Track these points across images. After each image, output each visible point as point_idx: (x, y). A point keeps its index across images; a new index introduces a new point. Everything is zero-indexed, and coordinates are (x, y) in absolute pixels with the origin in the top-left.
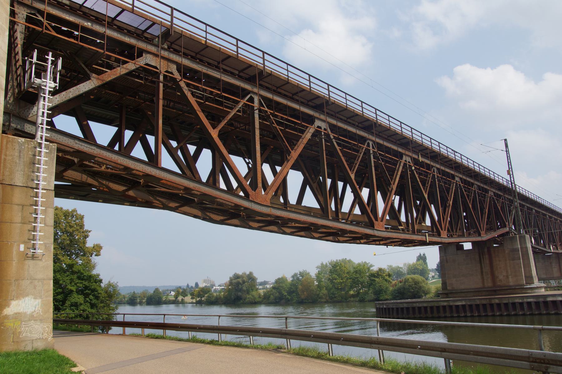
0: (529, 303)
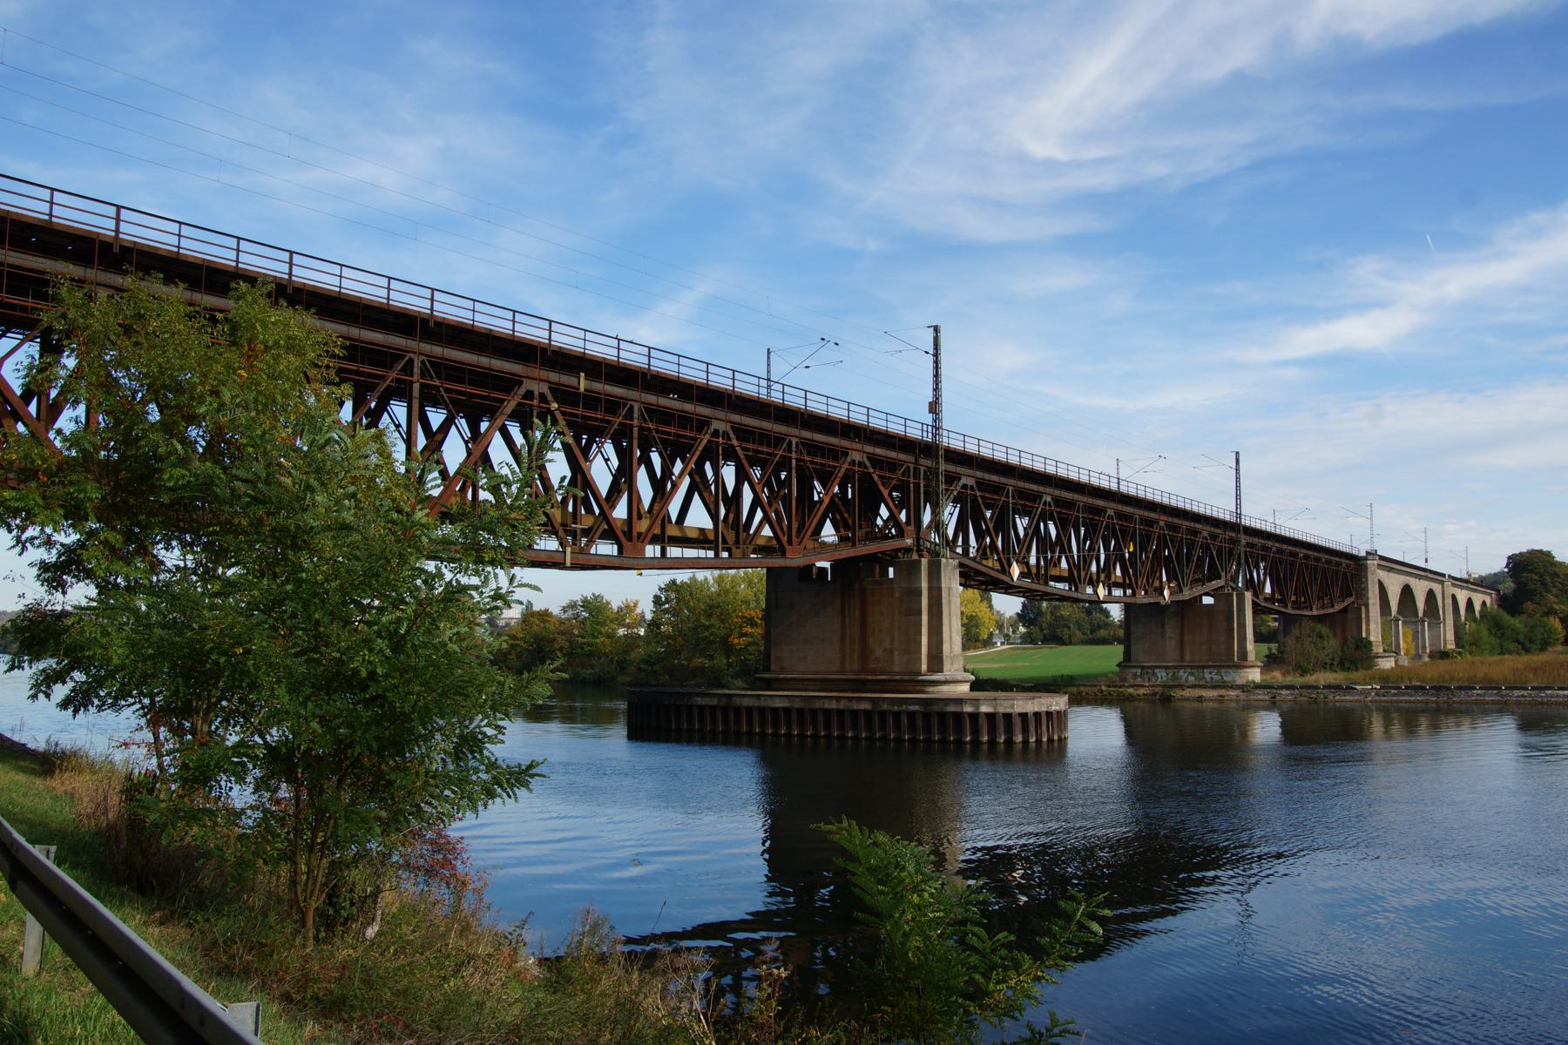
0: (912, 715)
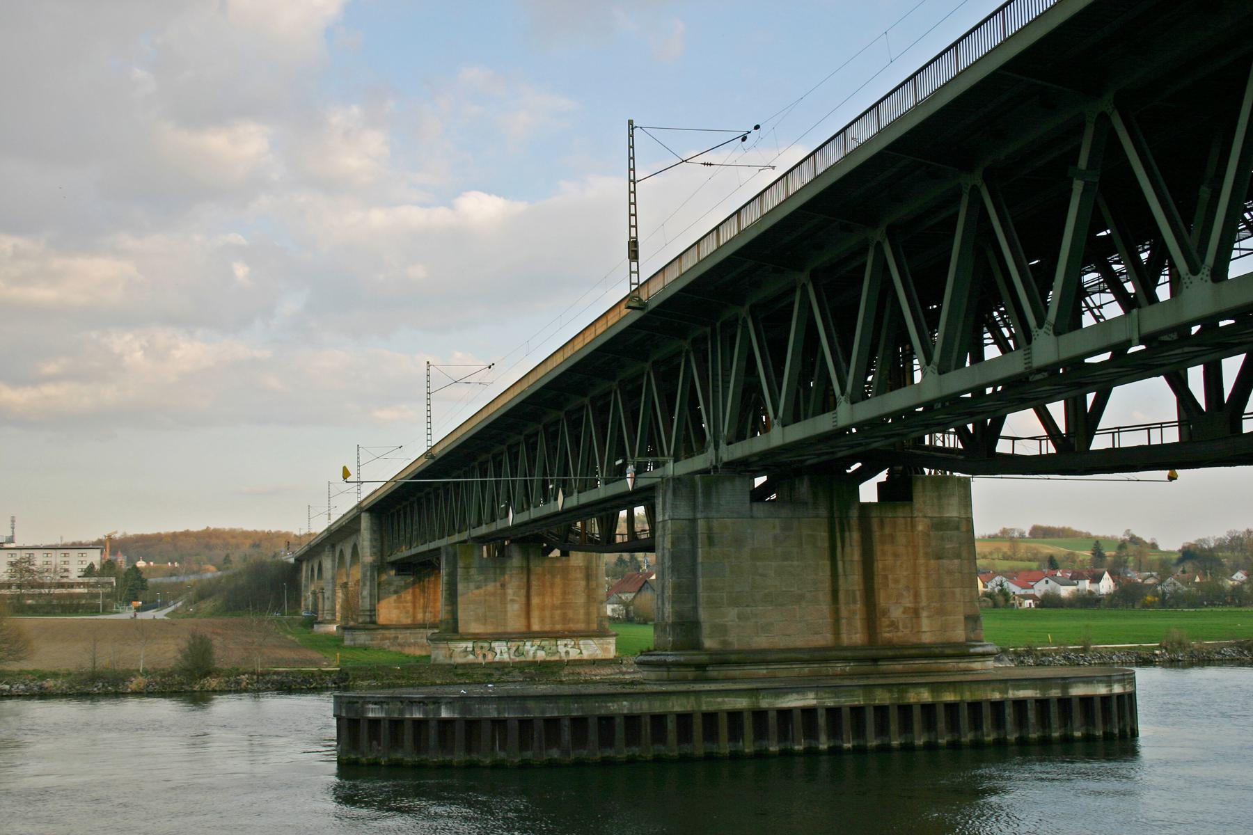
0: (1020, 704)
